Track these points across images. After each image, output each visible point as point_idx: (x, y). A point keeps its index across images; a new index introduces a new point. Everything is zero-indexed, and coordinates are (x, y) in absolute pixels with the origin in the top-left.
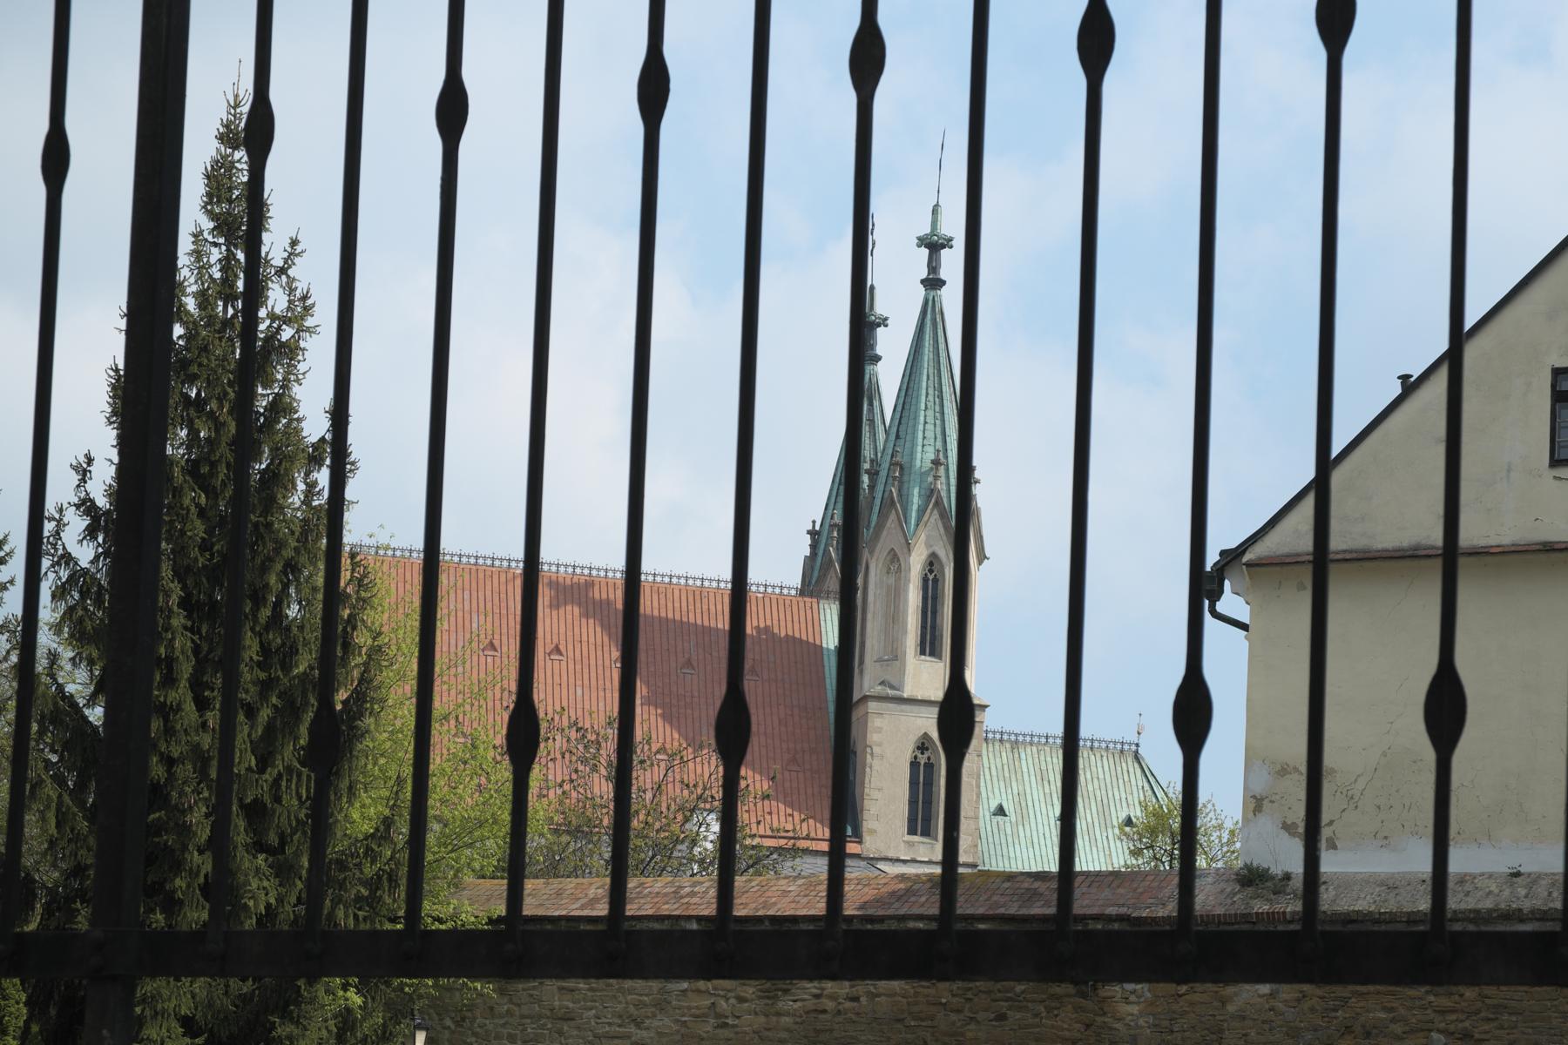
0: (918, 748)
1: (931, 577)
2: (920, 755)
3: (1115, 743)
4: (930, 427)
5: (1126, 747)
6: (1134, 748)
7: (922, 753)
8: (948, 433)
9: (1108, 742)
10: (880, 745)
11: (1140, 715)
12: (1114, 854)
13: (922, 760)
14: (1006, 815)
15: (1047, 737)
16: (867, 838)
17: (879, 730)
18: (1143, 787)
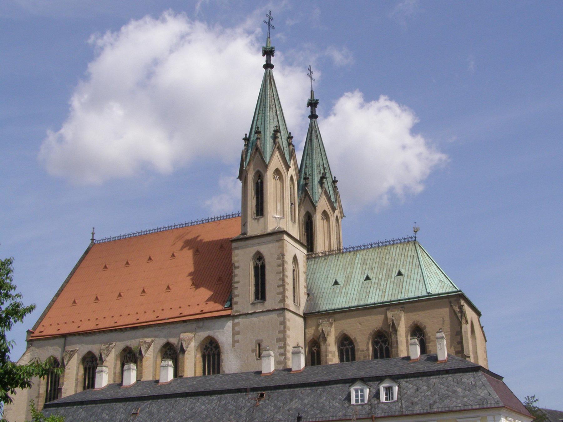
0: (258, 259)
1: (259, 181)
3: (404, 239)
4: (259, 120)
5: (410, 240)
6: (414, 239)
7: (260, 261)
8: (266, 120)
9: (401, 240)
10: (238, 261)
11: (415, 223)
13: (259, 264)
14: (339, 284)
15: (371, 245)
18: (413, 256)
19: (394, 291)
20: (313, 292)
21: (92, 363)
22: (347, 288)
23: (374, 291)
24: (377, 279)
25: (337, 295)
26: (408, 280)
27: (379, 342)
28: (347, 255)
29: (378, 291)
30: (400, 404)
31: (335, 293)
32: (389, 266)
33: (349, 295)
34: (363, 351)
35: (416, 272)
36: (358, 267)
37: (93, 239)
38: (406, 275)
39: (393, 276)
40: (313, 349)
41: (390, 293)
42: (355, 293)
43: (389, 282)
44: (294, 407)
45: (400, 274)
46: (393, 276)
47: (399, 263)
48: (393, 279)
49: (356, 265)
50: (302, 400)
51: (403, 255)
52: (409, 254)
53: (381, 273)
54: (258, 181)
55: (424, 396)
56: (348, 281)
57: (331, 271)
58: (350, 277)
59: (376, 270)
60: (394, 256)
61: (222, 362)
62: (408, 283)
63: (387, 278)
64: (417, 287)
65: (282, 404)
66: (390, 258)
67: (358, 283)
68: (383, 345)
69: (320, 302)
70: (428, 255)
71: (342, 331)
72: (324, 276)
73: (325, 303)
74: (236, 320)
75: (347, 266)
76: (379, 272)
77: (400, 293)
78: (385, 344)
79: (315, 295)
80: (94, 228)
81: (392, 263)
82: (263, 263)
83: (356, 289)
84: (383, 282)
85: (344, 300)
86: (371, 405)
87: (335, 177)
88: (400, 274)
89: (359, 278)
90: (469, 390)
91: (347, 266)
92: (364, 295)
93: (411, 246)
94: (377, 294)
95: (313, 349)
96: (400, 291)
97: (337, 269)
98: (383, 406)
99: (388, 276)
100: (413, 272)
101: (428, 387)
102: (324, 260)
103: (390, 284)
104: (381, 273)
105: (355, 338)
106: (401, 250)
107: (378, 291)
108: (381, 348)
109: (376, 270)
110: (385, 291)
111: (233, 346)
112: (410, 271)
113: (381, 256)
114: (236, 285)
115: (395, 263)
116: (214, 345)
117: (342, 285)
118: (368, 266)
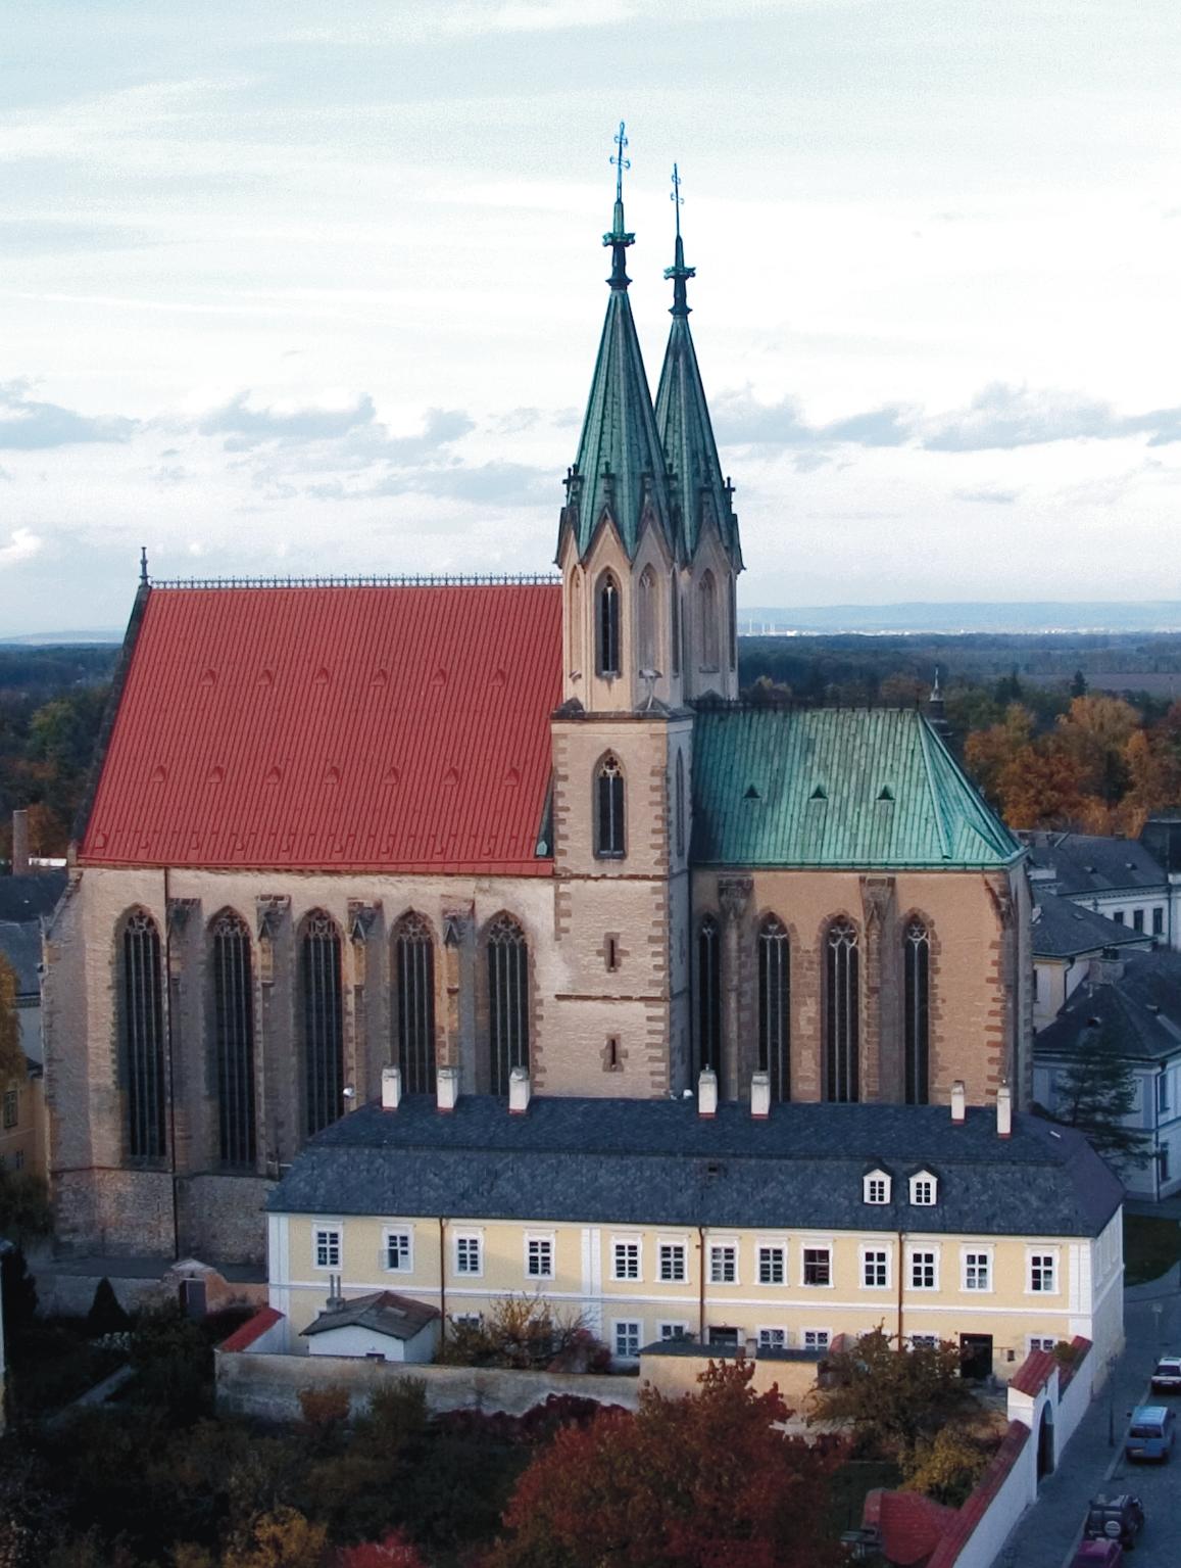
2: (608, 771)
12: (861, 833)
13: (611, 773)
16: (558, 858)
17: (564, 751)
19: (874, 837)
20: (704, 806)
21: (232, 929)
22: (777, 808)
23: (834, 828)
24: (838, 798)
25: (755, 824)
26: (904, 813)
27: (839, 936)
28: (769, 718)
29: (841, 828)
30: (941, 1212)
31: (752, 820)
32: (862, 768)
33: (781, 830)
34: (808, 951)
35: (919, 798)
36: (796, 759)
37: (144, 577)
38: (898, 800)
39: (872, 798)
40: (705, 931)
41: (867, 842)
42: (795, 826)
43: (863, 813)
44: (771, 1196)
45: (885, 795)
46: (872, 798)
47: (882, 765)
48: (871, 806)
49: (790, 751)
50: (783, 1184)
51: (891, 746)
52: (904, 746)
53: (846, 784)
54: (606, 590)
55: (977, 1202)
56: (776, 796)
57: (737, 756)
58: (780, 783)
59: (834, 776)
60: (871, 741)
61: (534, 966)
62: (903, 820)
63: (858, 800)
64: (922, 836)
65: (749, 1190)
66: (864, 747)
67: (798, 800)
68: (847, 942)
69: (720, 838)
70: (942, 751)
71: (768, 908)
72: (723, 767)
73: (732, 841)
74: (563, 888)
75: (771, 748)
76: (840, 778)
77: (887, 846)
78: (851, 942)
79: (709, 815)
80: (144, 548)
81: (869, 760)
82: (618, 773)
83: (796, 815)
84: (850, 809)
85: (773, 842)
86: (896, 1207)
87: (729, 479)
88: (885, 795)
89: (799, 789)
90: (1047, 1201)
91: (771, 748)
92: (813, 837)
93: (908, 719)
94: (840, 837)
95: (705, 931)
96: (887, 840)
97: (751, 753)
98: (915, 1212)
99: (861, 798)
100: (912, 797)
101: (983, 1185)
102: (721, 719)
103: (866, 817)
104: (846, 784)
105: (793, 925)
106: (886, 728)
107: (841, 828)
108: (842, 948)
109: (834, 776)
110: (857, 834)
111: (558, 939)
112: (906, 790)
113: (845, 738)
114: (562, 815)
115: (875, 764)
116: (513, 926)
117: (764, 800)
118: (817, 759)
